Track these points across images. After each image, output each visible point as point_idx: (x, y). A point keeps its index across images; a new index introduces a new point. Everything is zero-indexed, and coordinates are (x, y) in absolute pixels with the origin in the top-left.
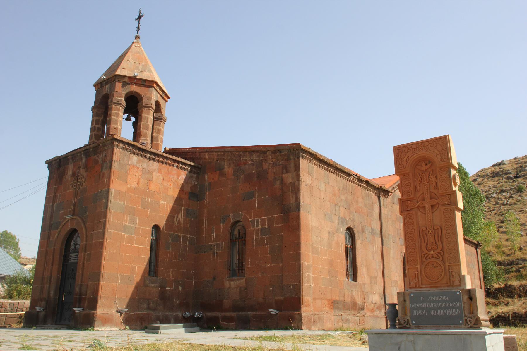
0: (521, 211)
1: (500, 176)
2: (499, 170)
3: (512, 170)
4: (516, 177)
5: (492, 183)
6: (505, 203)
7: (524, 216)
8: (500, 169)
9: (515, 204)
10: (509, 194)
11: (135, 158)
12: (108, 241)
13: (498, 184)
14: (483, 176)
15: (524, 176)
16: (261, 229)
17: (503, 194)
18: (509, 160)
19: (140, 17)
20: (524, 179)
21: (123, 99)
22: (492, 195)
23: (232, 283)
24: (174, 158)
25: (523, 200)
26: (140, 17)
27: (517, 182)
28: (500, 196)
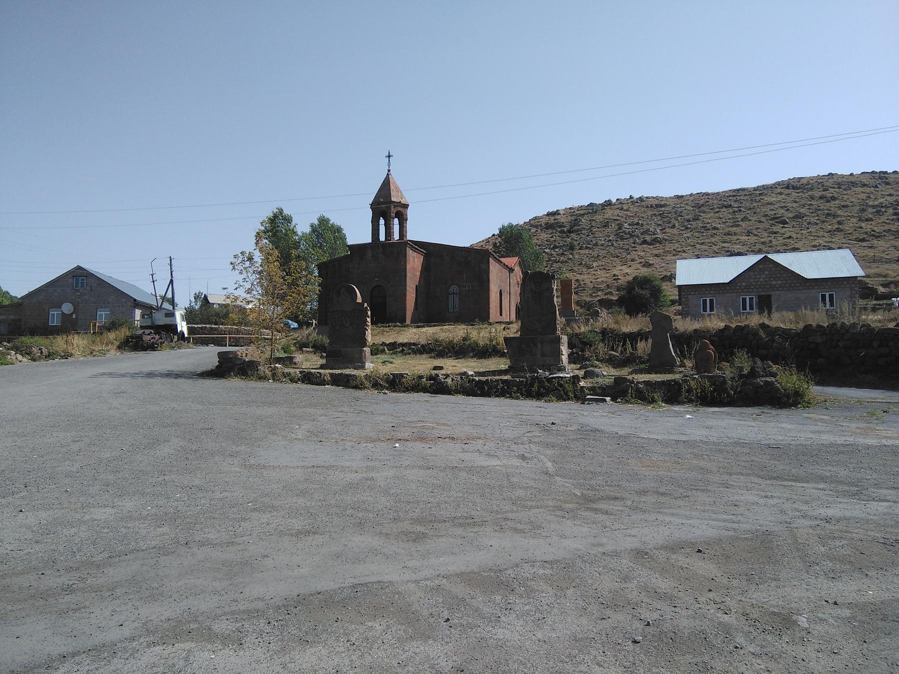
0: (571, 270)
1: (554, 229)
2: (554, 221)
3: (566, 223)
4: (569, 232)
5: (546, 236)
6: (557, 260)
7: (573, 275)
8: (555, 220)
9: (566, 262)
10: (561, 250)
11: (411, 251)
12: (407, 293)
13: (551, 237)
14: (536, 227)
15: (577, 231)
16: (468, 289)
17: (556, 250)
18: (564, 210)
19: (389, 156)
20: (577, 235)
21: (394, 215)
22: (545, 250)
23: (451, 315)
24: (421, 250)
25: (573, 259)
26: (389, 156)
27: (570, 238)
28: (553, 253)
